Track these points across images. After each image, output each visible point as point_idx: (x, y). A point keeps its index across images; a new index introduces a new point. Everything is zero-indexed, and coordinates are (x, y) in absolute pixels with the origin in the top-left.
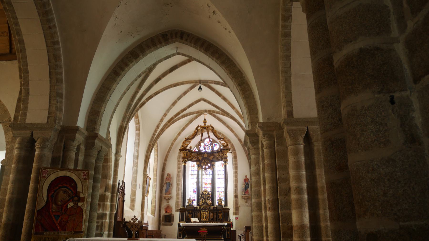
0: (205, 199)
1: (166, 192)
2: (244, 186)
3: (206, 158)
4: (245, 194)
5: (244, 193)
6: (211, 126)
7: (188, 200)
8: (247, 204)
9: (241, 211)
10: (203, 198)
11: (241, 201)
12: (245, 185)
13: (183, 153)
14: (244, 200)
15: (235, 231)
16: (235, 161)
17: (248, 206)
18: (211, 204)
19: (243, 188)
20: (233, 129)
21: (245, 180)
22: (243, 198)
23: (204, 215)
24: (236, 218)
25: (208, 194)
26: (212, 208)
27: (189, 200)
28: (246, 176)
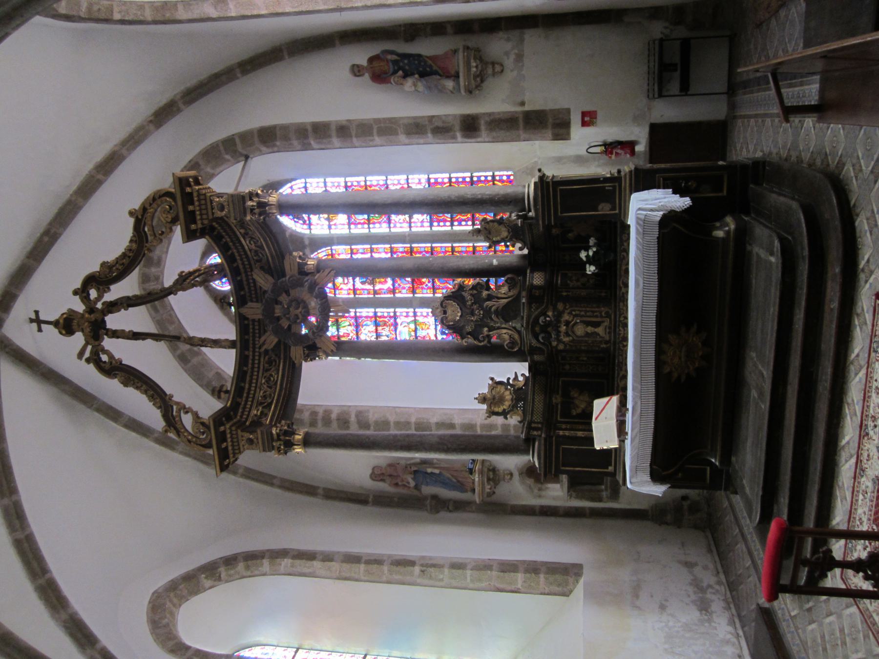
0: (488, 312)
1: (460, 486)
2: (410, 82)
3: (268, 311)
4: (456, 76)
5: (450, 84)
6: (82, 292)
7: (492, 413)
8: (509, 62)
9: (541, 96)
10: (479, 325)
11: (495, 102)
12: (406, 76)
13: (238, 451)
14: (490, 82)
15: (655, 130)
16: (286, 138)
17: (519, 57)
18: (511, 284)
19: (421, 86)
20: (99, 157)
21: (379, 78)
22: (476, 86)
23: (580, 330)
24: (584, 124)
25: (456, 296)
26: (538, 279)
27: (491, 402)
28: (357, 71)
